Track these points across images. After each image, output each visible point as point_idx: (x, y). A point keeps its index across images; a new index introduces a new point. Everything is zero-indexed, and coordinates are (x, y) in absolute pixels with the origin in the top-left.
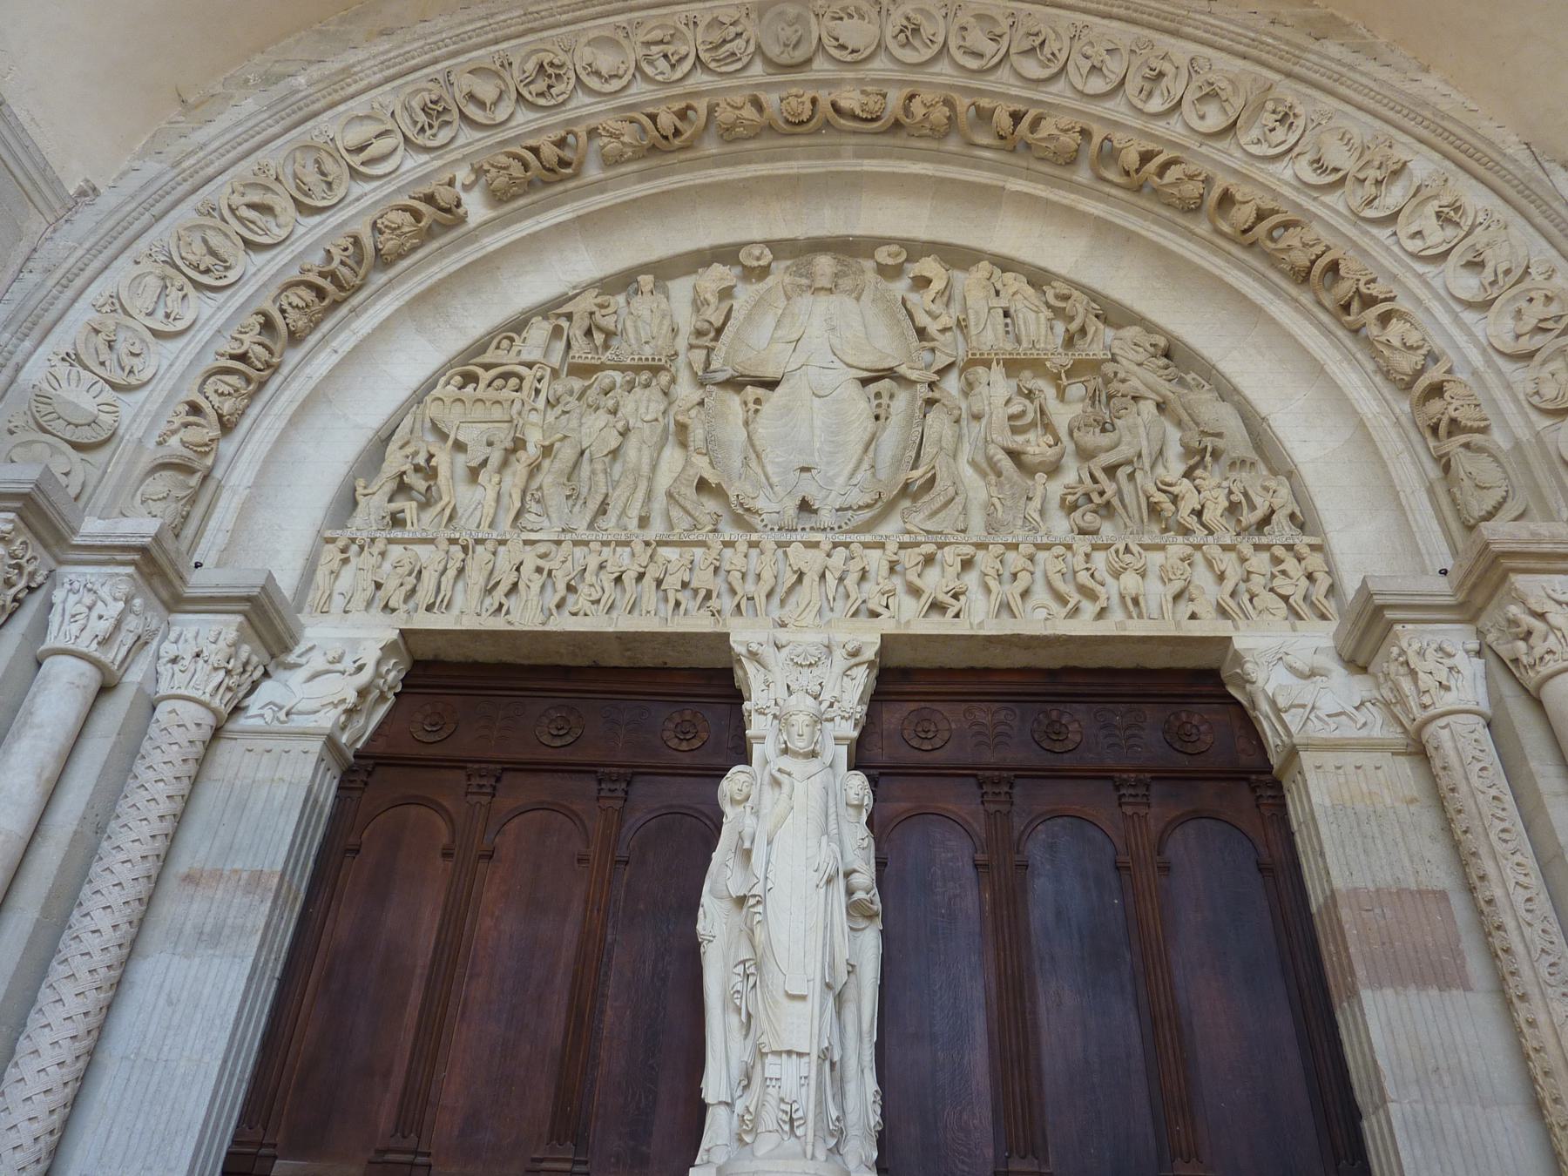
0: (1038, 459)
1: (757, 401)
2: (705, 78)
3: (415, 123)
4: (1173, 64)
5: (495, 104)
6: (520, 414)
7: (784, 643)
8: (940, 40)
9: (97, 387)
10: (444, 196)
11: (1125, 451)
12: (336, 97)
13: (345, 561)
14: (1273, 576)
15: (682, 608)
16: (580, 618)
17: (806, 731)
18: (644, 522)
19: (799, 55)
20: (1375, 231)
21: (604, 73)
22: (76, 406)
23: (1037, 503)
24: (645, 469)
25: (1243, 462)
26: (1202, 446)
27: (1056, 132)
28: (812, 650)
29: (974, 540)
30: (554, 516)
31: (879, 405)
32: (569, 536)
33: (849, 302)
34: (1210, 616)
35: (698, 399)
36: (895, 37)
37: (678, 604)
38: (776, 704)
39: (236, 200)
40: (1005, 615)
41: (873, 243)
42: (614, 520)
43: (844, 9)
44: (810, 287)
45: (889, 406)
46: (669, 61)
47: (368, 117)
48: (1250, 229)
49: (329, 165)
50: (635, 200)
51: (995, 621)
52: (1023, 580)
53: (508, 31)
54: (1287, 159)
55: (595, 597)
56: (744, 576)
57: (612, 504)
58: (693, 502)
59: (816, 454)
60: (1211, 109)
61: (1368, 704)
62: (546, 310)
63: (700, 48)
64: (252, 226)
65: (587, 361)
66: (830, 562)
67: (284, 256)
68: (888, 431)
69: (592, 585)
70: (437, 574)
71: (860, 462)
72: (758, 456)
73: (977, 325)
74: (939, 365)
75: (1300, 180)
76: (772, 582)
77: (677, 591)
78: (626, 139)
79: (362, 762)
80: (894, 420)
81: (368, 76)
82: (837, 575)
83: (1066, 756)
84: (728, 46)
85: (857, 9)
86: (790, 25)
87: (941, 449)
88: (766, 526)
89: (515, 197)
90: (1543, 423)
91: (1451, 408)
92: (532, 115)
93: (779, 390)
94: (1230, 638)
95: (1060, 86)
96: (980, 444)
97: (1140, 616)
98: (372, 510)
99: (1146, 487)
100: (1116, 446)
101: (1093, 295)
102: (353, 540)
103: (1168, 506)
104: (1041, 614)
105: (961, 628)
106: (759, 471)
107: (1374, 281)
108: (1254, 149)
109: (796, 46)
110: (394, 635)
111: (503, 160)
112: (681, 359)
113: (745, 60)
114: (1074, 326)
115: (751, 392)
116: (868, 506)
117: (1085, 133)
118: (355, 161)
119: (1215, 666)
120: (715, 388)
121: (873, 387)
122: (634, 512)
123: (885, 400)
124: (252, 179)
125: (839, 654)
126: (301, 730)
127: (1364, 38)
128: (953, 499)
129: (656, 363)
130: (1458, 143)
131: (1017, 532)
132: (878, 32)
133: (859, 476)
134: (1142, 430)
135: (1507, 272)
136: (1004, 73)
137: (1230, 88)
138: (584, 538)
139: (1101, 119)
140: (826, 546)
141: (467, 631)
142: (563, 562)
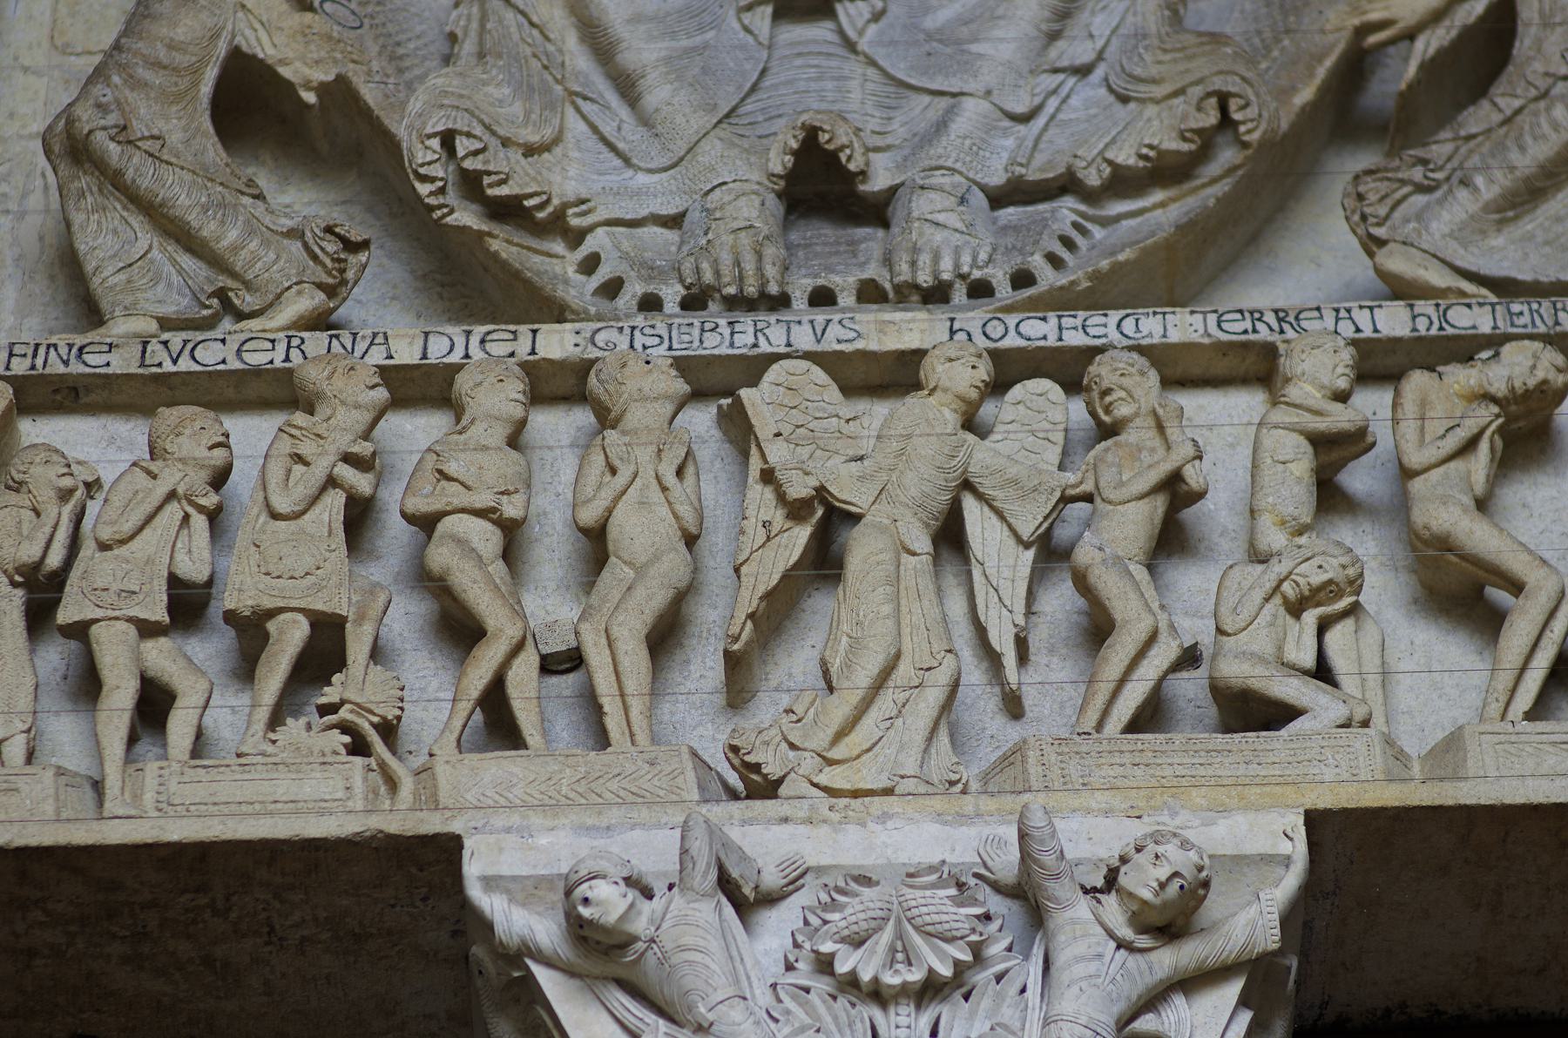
7: (772, 879)
15: (180, 726)
28: (938, 905)
56: (513, 535)
58: (205, 174)
66: (982, 456)
76: (675, 565)
77: (147, 630)
88: (612, 289)
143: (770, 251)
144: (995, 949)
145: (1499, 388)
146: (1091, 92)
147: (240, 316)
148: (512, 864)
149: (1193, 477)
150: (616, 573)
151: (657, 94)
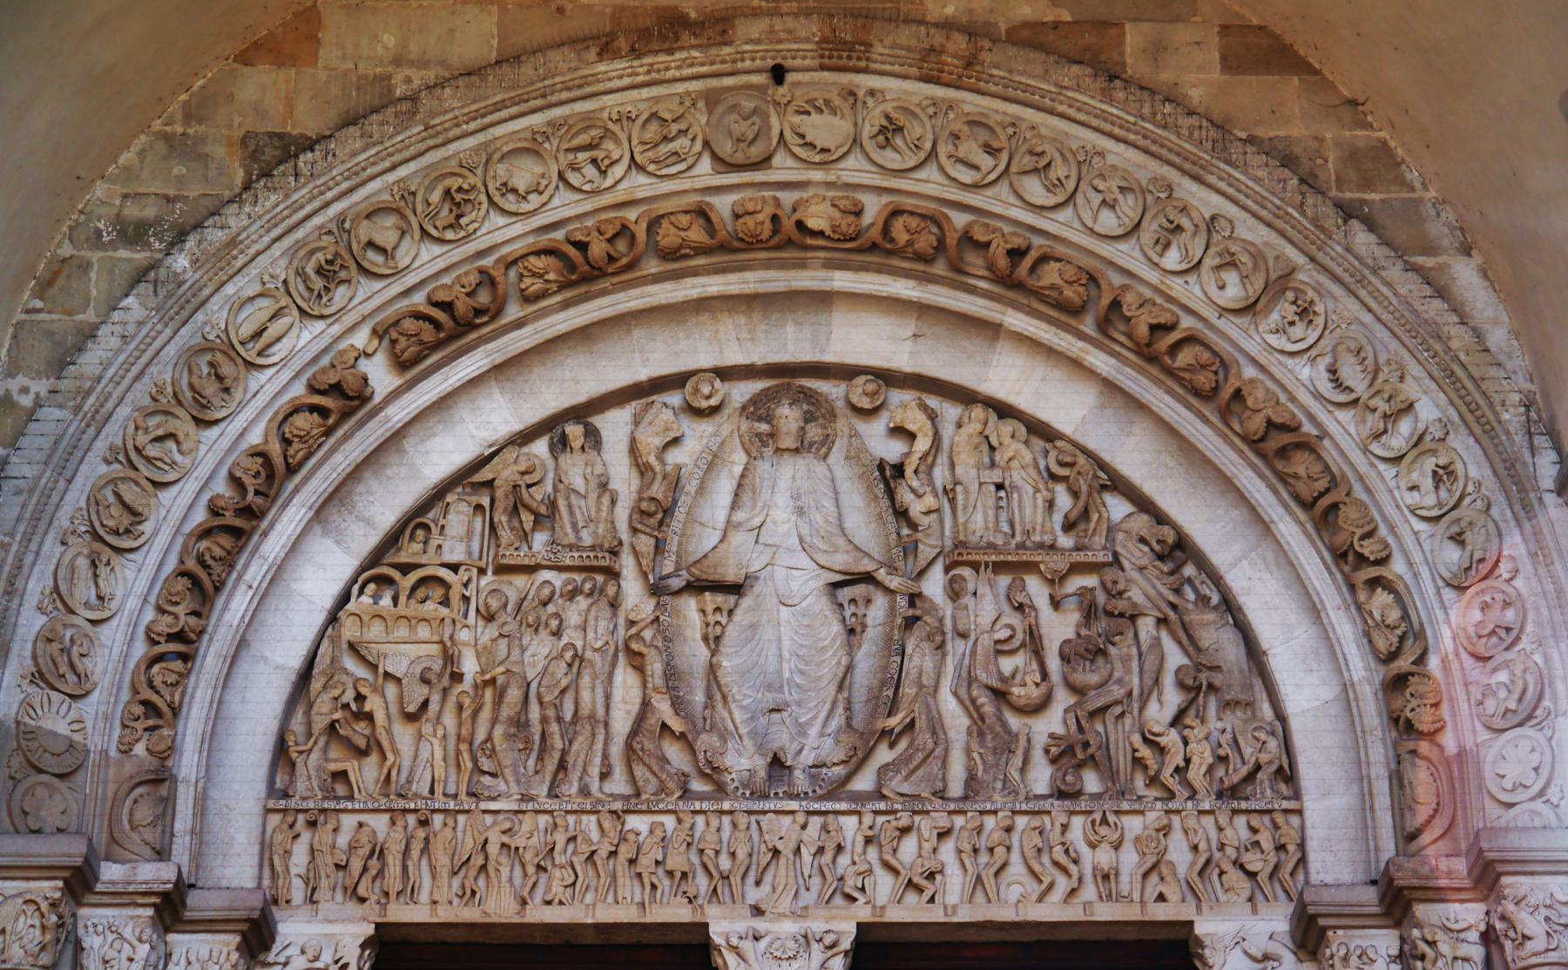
0: (1022, 702)
1: (718, 609)
2: (642, 179)
3: (311, 290)
4: (1192, 219)
5: (394, 248)
6: (451, 637)
8: (928, 145)
9: (65, 706)
11: (1117, 692)
12: (222, 276)
18: (604, 776)
19: (756, 152)
20: (1382, 467)
21: (521, 192)
22: (56, 734)
23: (1018, 761)
24: (601, 712)
25: (1237, 703)
27: (1059, 281)
30: (511, 779)
31: (854, 614)
32: (530, 806)
36: (875, 136)
39: (142, 439)
40: (979, 895)
41: (847, 373)
42: (576, 784)
43: (810, 101)
44: (772, 435)
46: (599, 168)
47: (261, 295)
49: (227, 369)
53: (407, 154)
54: (1306, 357)
60: (1231, 277)
63: (637, 151)
64: (159, 464)
67: (190, 487)
71: (834, 703)
72: (724, 697)
73: (965, 507)
76: (746, 862)
78: (551, 276)
81: (254, 242)
82: (813, 850)
84: (672, 146)
85: (827, 102)
86: (746, 118)
87: (921, 686)
89: (426, 357)
90: (1484, 735)
91: (1410, 706)
92: (438, 249)
94: (1192, 922)
95: (1066, 214)
96: (964, 674)
98: (313, 773)
101: (1102, 465)
104: (1014, 893)
105: (935, 915)
106: (726, 714)
107: (1369, 535)
108: (1273, 340)
109: (751, 143)
110: (370, 930)
111: (409, 325)
112: (626, 550)
113: (690, 161)
116: (843, 762)
117: (1093, 279)
118: (250, 355)
121: (845, 594)
122: (595, 771)
124: (152, 406)
125: (815, 947)
127: (1412, 189)
128: (933, 751)
130: (1463, 392)
131: (997, 797)
132: (852, 130)
134: (1135, 664)
135: (1481, 561)
136: (1003, 189)
137: (1250, 265)
138: (547, 807)
139: (1112, 264)
148: (718, 929)
151: (746, 742)
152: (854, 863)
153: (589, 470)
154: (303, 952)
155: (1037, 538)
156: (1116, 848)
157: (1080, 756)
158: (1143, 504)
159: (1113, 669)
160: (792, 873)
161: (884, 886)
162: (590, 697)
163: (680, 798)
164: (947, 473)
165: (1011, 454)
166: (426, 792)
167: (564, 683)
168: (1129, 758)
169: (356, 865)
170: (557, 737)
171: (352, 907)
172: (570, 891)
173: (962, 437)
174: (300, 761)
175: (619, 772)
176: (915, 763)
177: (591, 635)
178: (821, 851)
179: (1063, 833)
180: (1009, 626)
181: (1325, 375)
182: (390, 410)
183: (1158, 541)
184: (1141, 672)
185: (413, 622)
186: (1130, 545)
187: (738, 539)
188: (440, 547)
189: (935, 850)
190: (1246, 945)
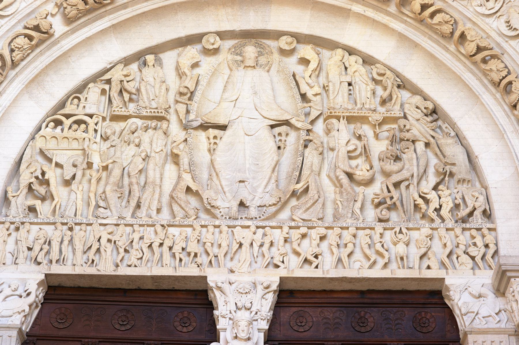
0: (361, 178)
1: (215, 137)
6: (88, 146)
7: (233, 282)
10: (44, 26)
11: (405, 174)
13: (9, 235)
14: (470, 246)
15: (183, 262)
16: (132, 268)
17: (246, 329)
18: (159, 211)
23: (358, 205)
24: (158, 181)
25: (464, 180)
26: (445, 171)
28: (247, 286)
29: (327, 225)
30: (113, 209)
31: (280, 140)
32: (122, 222)
33: (265, 74)
34: (436, 268)
35: (184, 139)
37: (181, 260)
38: (230, 313)
40: (340, 266)
41: (277, 35)
42: (144, 212)
44: (242, 62)
45: (285, 141)
48: (474, 55)
50: (144, 13)
51: (335, 270)
52: (350, 246)
54: (495, 17)
55: (140, 256)
56: (212, 244)
57: (143, 203)
59: (247, 172)
61: (503, 311)
62: (95, 79)
65: (121, 113)
66: (255, 237)
68: (285, 155)
69: (137, 250)
70: (58, 244)
71: (270, 178)
72: (217, 175)
74: (312, 117)
75: (499, 30)
76: (226, 248)
79: (31, 338)
80: (288, 148)
82: (259, 244)
83: (367, 334)
87: (312, 171)
88: (222, 216)
89: (79, 18)
93: (228, 132)
96: (333, 166)
97: (403, 267)
98: (19, 206)
99: (414, 195)
100: (401, 170)
101: (398, 75)
102: (12, 223)
103: (423, 206)
104: (357, 265)
105: (318, 274)
106: (217, 182)
108: (479, 9)
110: (43, 277)
112: (172, 111)
114: (385, 95)
115: (212, 132)
116: (274, 204)
119: (439, 289)
120: (192, 131)
121: (277, 130)
122: (154, 208)
123: (283, 138)
125: (260, 288)
126: (6, 326)
128: (318, 200)
129: (161, 115)
133: (269, 187)
134: (415, 161)
138: (130, 222)
140: (253, 229)
141: (78, 275)
142: (121, 236)
143: (237, 213)
144: (252, 290)
145: (301, 233)
146: (268, 195)
147: (189, 218)
148: (212, 279)
149: (273, 241)
150: (221, 248)
151: (227, 194)
152: (279, 250)
153: (156, 75)
154: (9, 287)
155: (367, 106)
156: (407, 245)
157: (389, 202)
158: (416, 91)
159: (404, 164)
160: (248, 254)
161: (294, 261)
162: (153, 174)
163: (195, 219)
164: (324, 79)
165: (355, 70)
166: (73, 216)
167: (141, 167)
168: (412, 205)
169: (37, 248)
170: (136, 191)
171: (34, 267)
172: (139, 261)
173: (332, 62)
174: (13, 200)
175: (166, 212)
176: (309, 205)
177: (154, 146)
178: (261, 246)
179: (381, 238)
180: (354, 144)
181: (505, 25)
182: (63, 43)
183: (425, 108)
184: (418, 165)
185: (70, 140)
186: (412, 109)
187: (224, 105)
188: (84, 107)
189: (318, 245)
190: (469, 289)
